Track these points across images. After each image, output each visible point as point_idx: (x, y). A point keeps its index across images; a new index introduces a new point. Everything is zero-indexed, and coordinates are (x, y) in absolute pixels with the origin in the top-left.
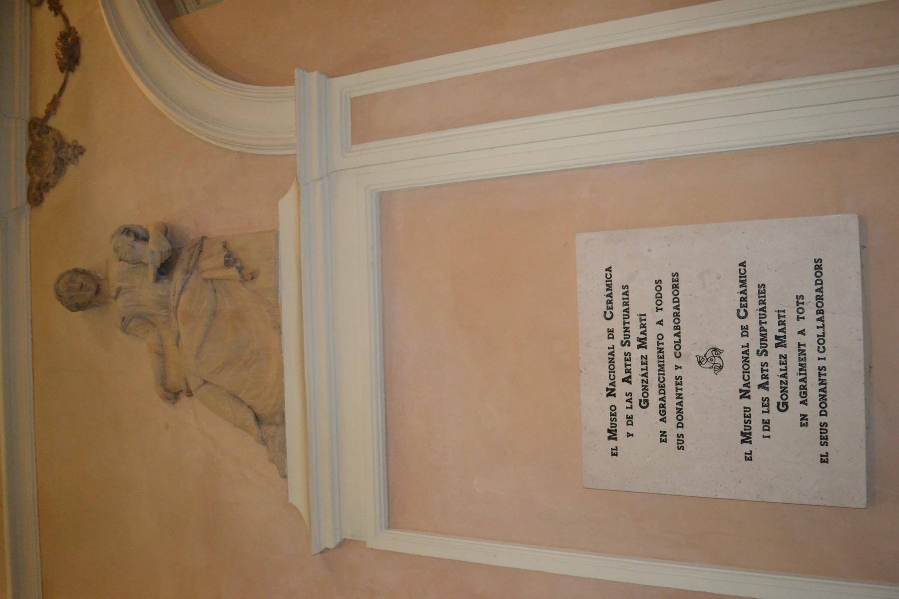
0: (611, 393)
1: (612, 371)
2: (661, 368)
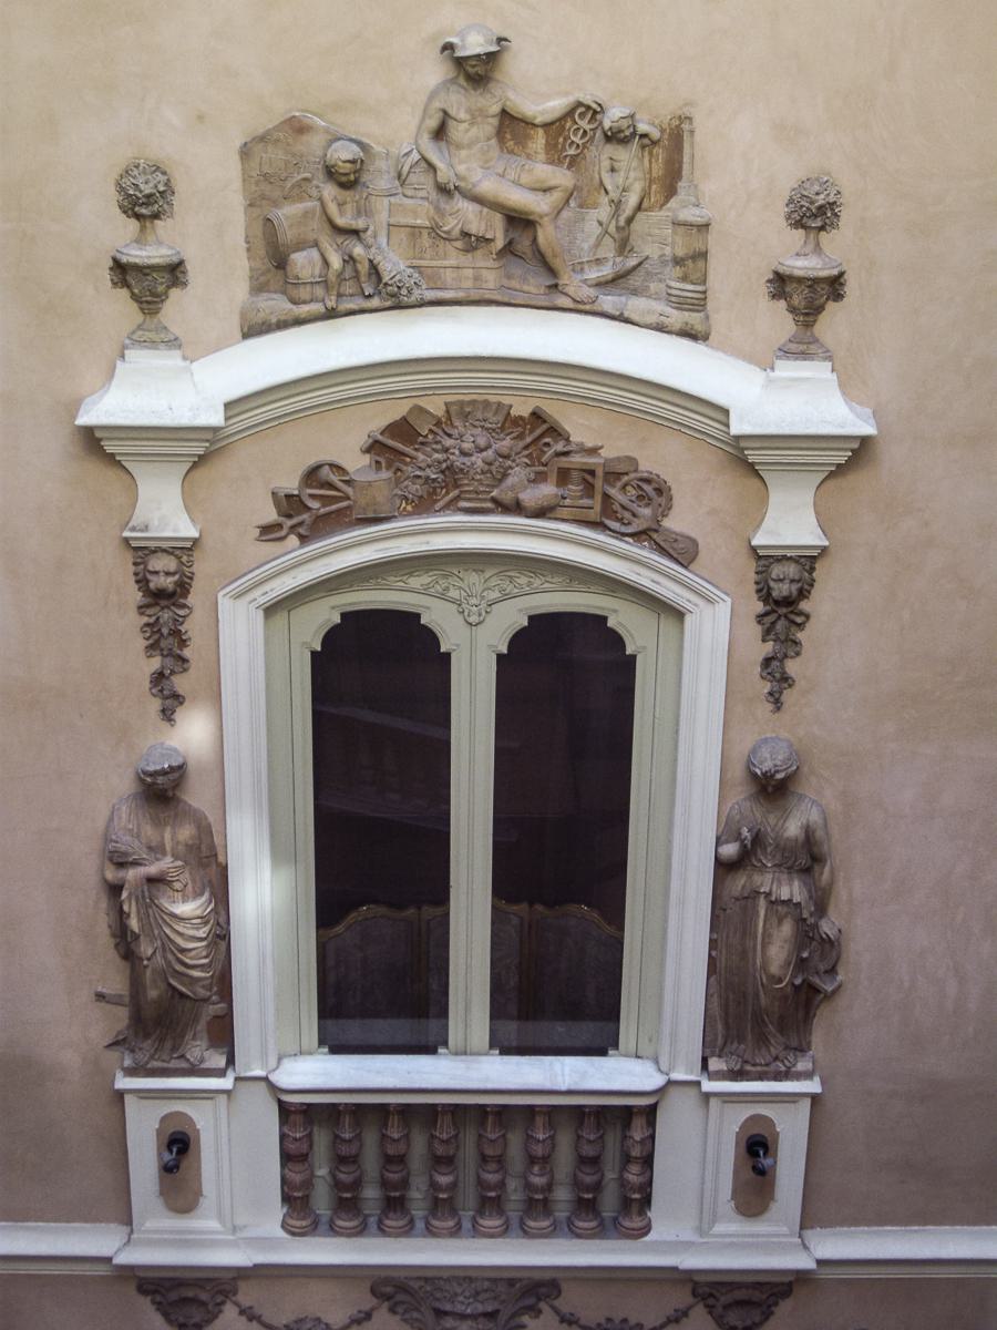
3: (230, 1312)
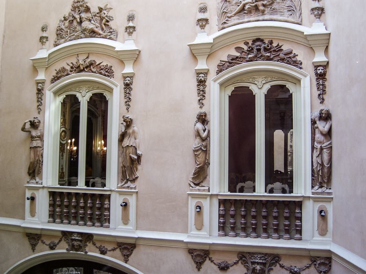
3: (208, 259)
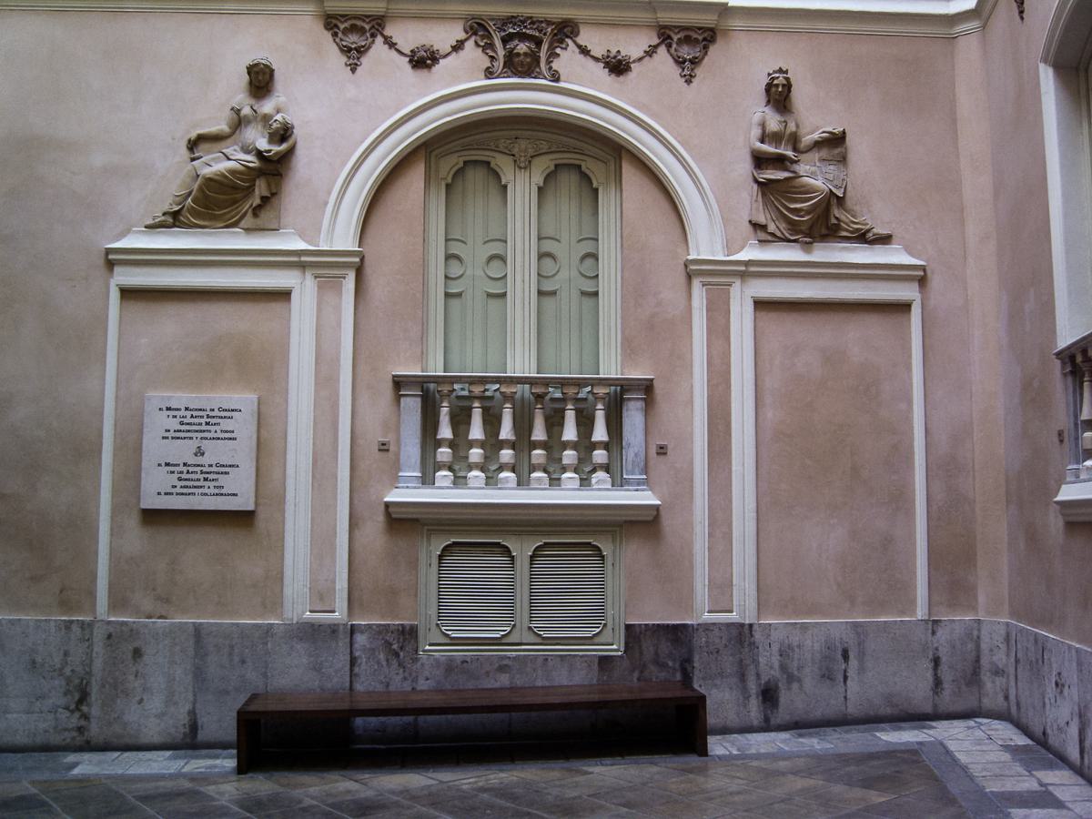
0: (187, 409)
1: (196, 410)
2: (197, 431)
3: (379, 39)
